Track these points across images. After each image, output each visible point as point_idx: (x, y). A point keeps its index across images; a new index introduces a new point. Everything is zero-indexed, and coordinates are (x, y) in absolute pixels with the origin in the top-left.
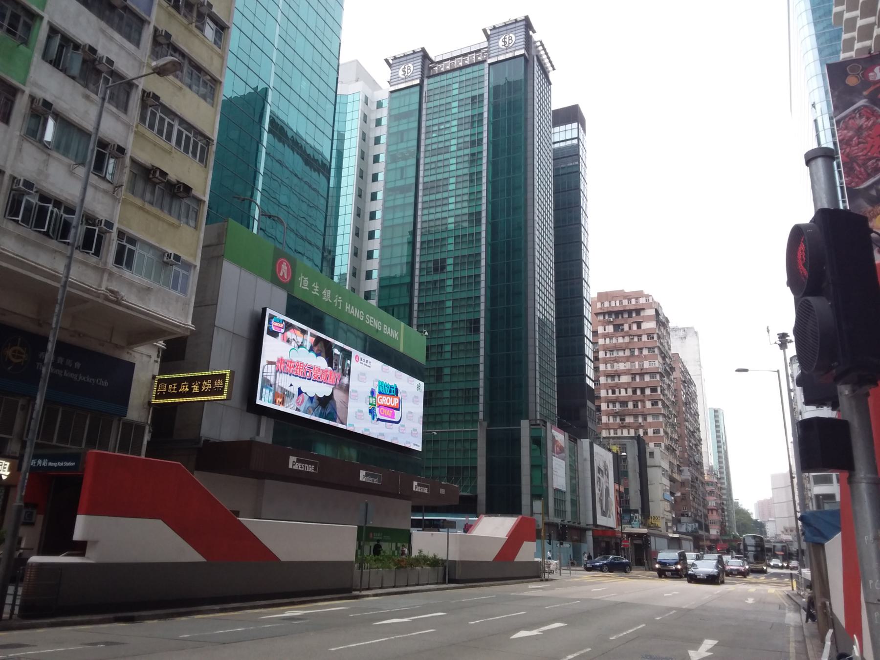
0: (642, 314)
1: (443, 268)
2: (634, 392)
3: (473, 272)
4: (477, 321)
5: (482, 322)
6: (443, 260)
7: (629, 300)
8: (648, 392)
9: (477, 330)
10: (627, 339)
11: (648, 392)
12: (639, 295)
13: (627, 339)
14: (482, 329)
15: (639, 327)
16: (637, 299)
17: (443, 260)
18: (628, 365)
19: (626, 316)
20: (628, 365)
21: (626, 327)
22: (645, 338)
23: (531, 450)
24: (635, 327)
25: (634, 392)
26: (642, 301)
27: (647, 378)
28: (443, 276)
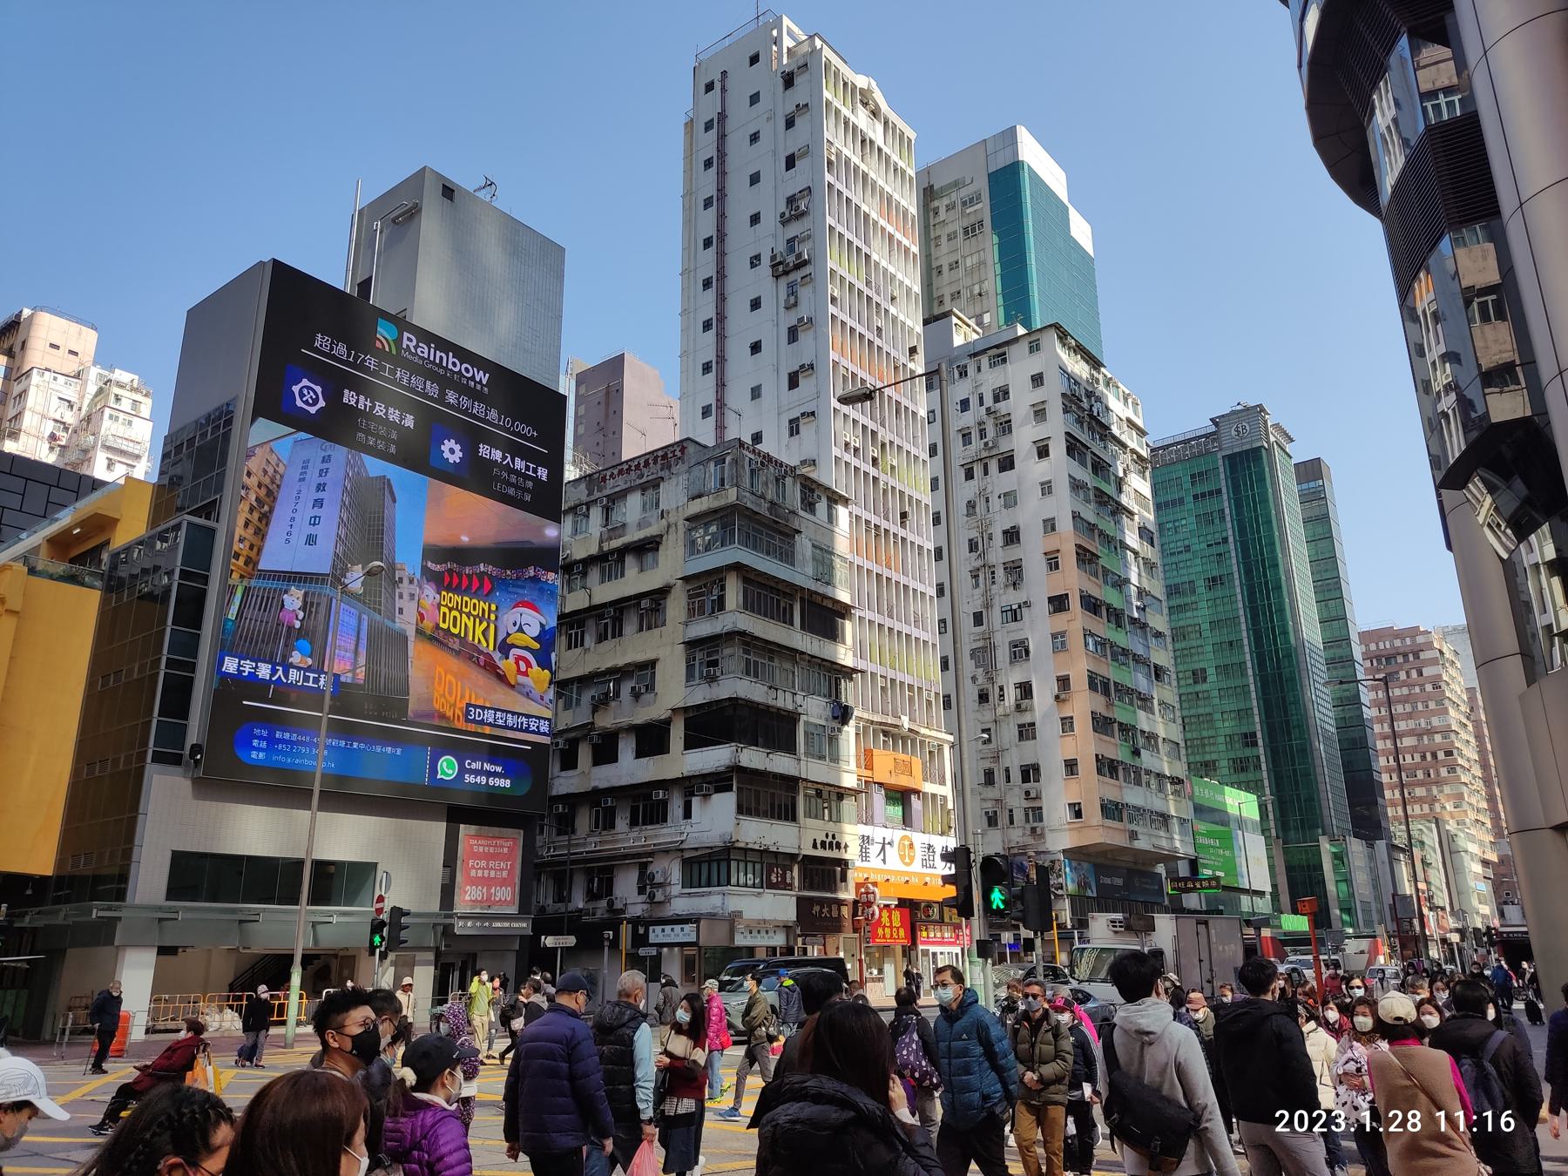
0: (1422, 656)
1: (1205, 680)
2: (1424, 757)
3: (1238, 682)
4: (1254, 735)
5: (1259, 735)
6: (1204, 671)
7: (1403, 639)
8: (1441, 755)
9: (1255, 744)
10: (1405, 691)
11: (1441, 755)
12: (1414, 632)
13: (1405, 691)
14: (1260, 742)
15: (1420, 674)
16: (1413, 637)
17: (1204, 671)
18: (1411, 724)
19: (1400, 659)
20: (1411, 724)
21: (1403, 675)
22: (1429, 688)
23: (1334, 866)
24: (1414, 674)
25: (1424, 757)
26: (1420, 639)
27: (1438, 738)
28: (1205, 687)
